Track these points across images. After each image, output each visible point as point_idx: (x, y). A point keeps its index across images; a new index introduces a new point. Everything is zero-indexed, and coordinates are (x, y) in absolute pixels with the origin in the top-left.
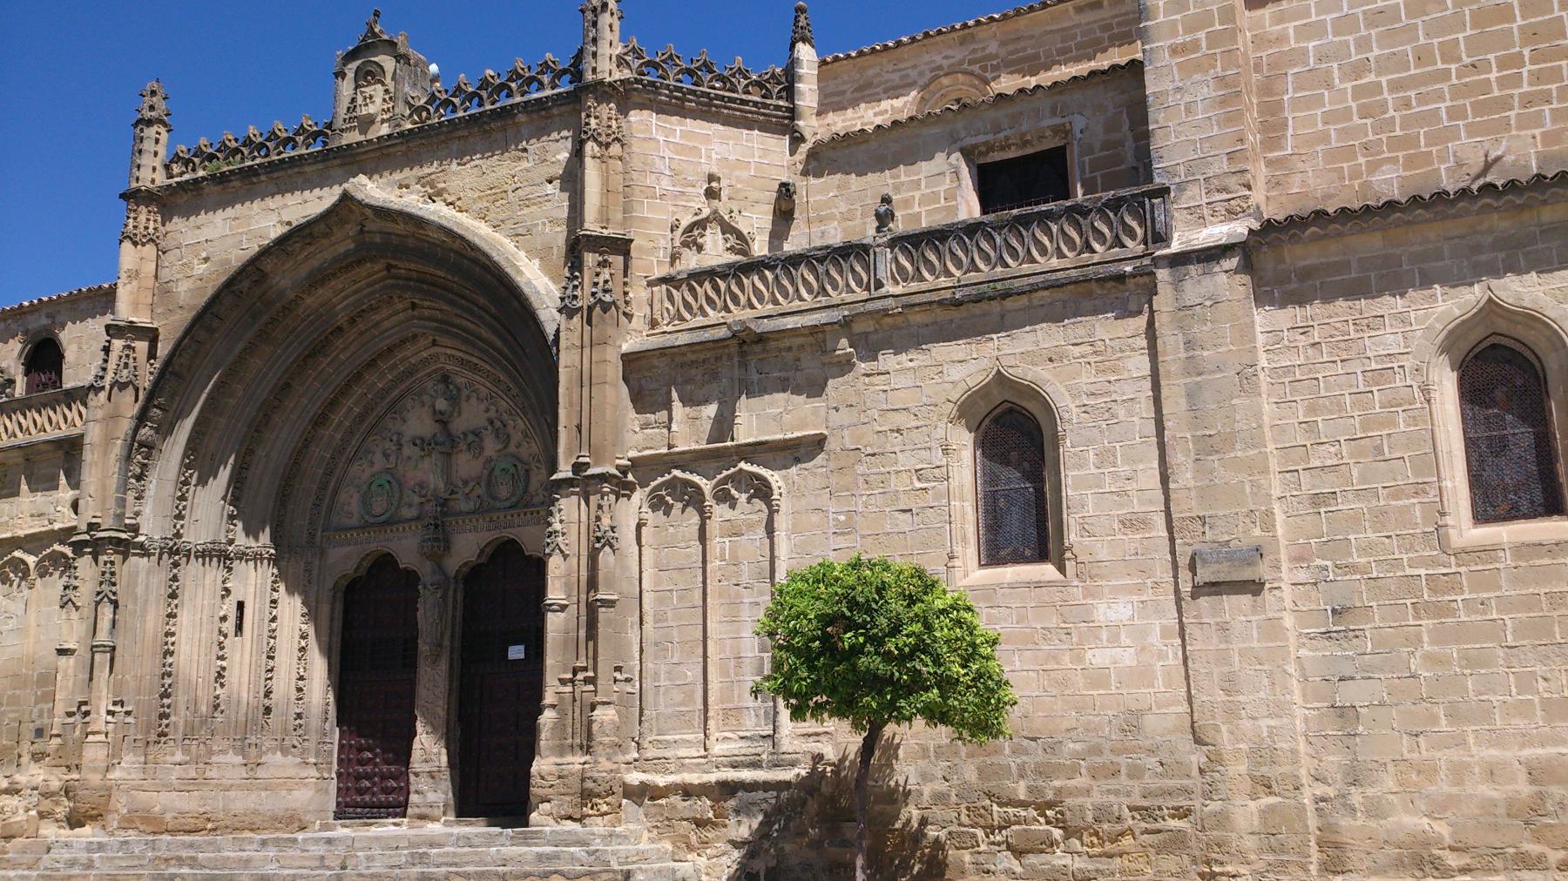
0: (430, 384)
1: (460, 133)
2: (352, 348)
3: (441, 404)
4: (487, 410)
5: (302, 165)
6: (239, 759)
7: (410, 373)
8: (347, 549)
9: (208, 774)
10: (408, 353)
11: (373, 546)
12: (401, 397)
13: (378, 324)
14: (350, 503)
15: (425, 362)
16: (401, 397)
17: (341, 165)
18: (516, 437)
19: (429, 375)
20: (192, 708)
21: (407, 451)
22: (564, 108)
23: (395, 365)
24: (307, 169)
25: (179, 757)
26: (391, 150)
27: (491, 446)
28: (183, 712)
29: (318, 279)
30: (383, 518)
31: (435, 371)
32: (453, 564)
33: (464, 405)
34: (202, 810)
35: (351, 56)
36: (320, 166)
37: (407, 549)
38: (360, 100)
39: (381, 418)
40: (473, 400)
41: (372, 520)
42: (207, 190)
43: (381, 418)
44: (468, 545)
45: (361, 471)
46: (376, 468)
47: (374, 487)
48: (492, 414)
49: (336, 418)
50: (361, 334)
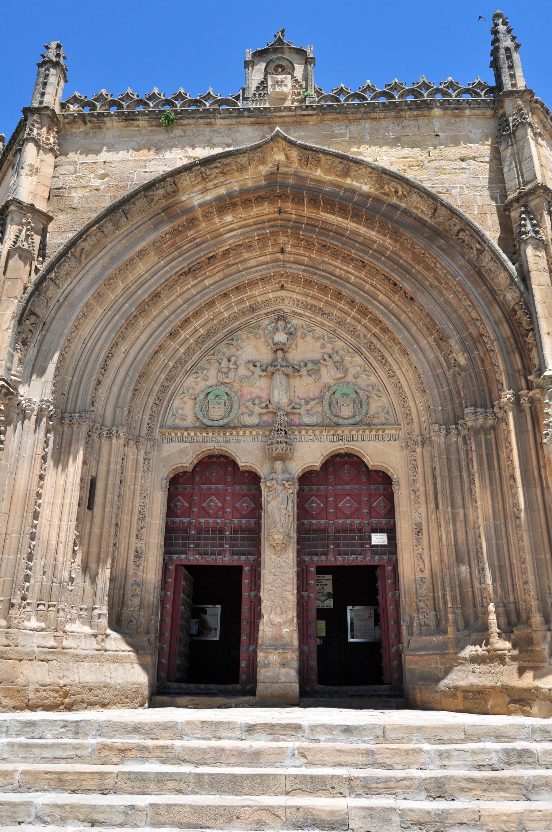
0: (266, 322)
1: (377, 115)
2: (217, 278)
3: (281, 337)
4: (323, 347)
5: (214, 117)
6: (87, 630)
7: (253, 309)
8: (182, 446)
9: (65, 643)
10: (256, 292)
11: (210, 445)
12: (238, 329)
13: (244, 261)
14: (185, 409)
15: (267, 302)
16: (238, 329)
17: (252, 124)
18: (352, 371)
19: (267, 314)
20: (50, 573)
21: (242, 371)
22: (477, 112)
23: (242, 301)
24: (219, 121)
25: (34, 623)
26: (306, 118)
27: (328, 375)
28: (39, 576)
29: (225, 204)
30: (221, 423)
31: (273, 312)
32: (297, 467)
33: (300, 340)
34: (62, 682)
35: (260, 54)
36: (233, 121)
37: (247, 452)
38: (270, 83)
39: (218, 343)
40: (309, 338)
41: (210, 423)
42: (109, 124)
43: (218, 343)
44: (311, 453)
45: (195, 383)
46: (212, 381)
47: (210, 397)
48: (328, 350)
49: (184, 334)
50: (228, 266)
